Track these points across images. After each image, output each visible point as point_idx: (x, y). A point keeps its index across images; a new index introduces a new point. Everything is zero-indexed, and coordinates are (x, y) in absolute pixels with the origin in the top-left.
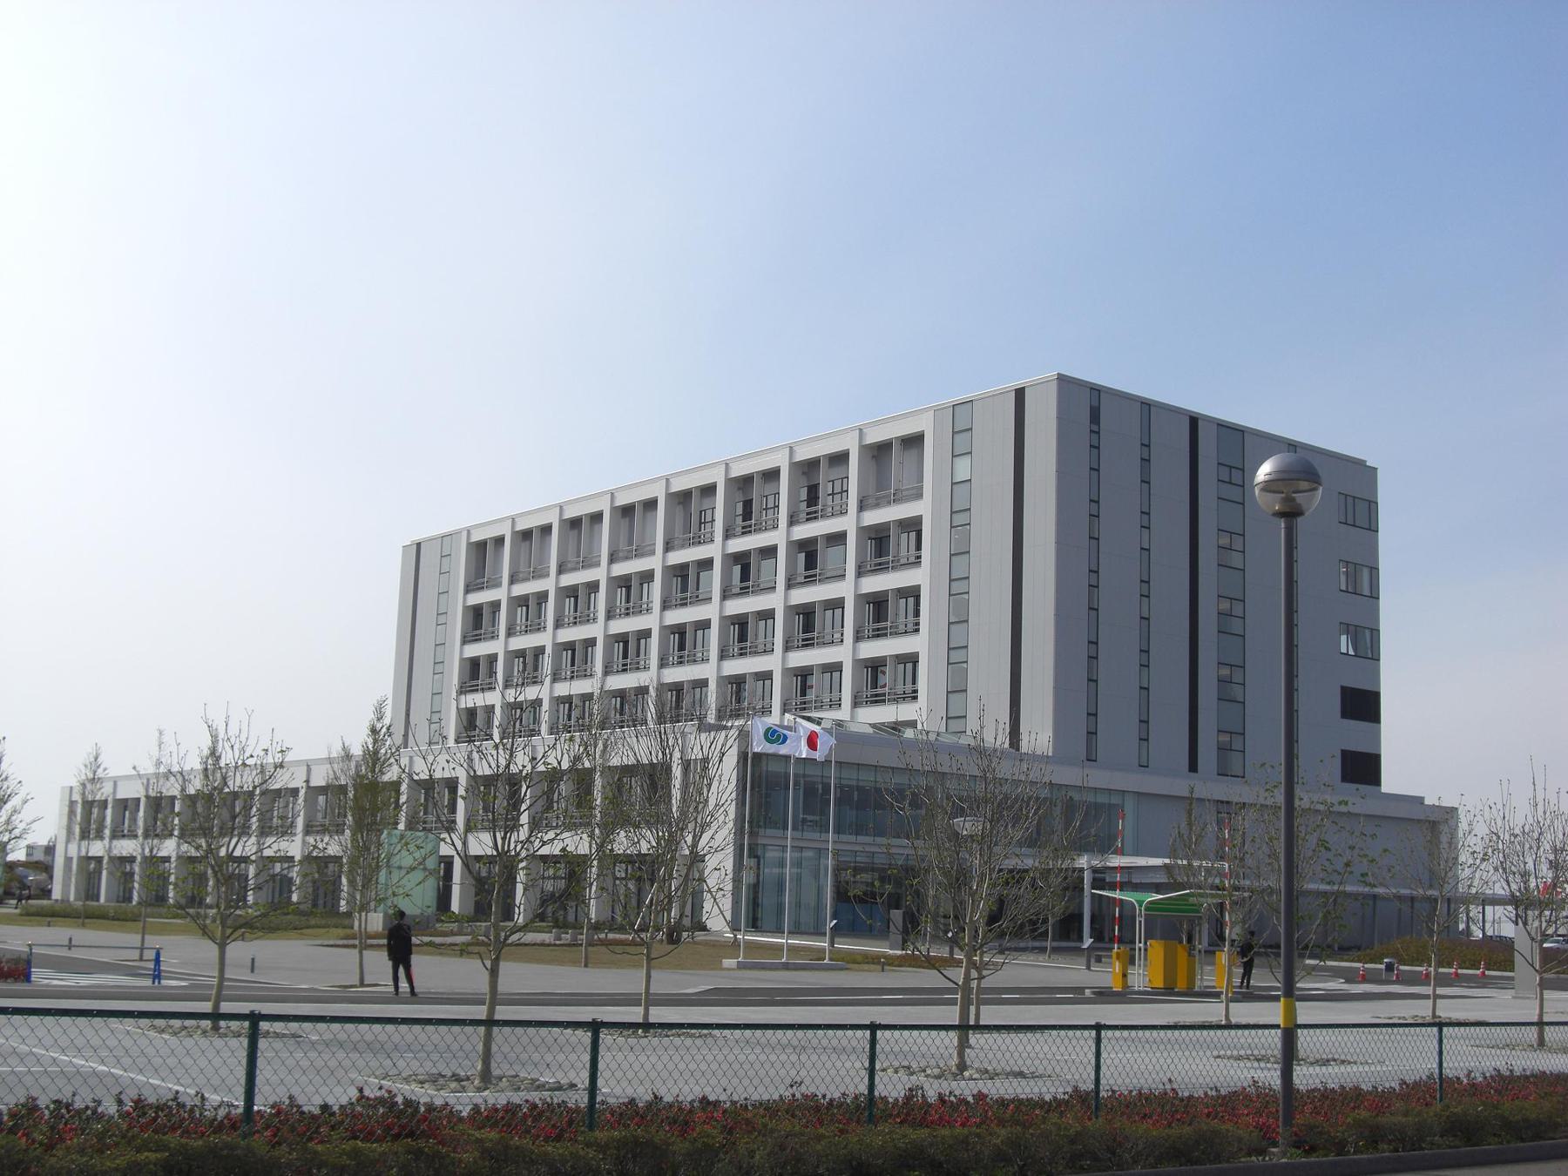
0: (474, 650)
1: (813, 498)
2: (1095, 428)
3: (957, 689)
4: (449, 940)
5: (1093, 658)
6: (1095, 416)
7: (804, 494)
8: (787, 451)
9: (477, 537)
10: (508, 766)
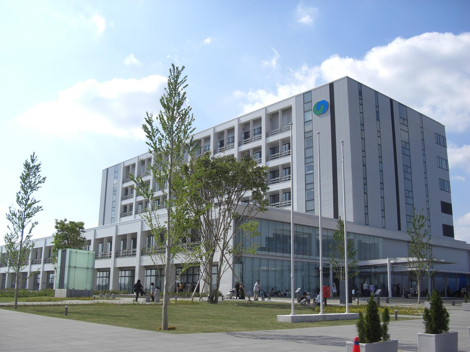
0: (125, 202)
1: (222, 144)
2: (361, 97)
3: (310, 198)
4: (60, 303)
5: (365, 184)
6: (360, 93)
7: (219, 144)
8: (237, 120)
9: (127, 164)
10: (204, 216)
